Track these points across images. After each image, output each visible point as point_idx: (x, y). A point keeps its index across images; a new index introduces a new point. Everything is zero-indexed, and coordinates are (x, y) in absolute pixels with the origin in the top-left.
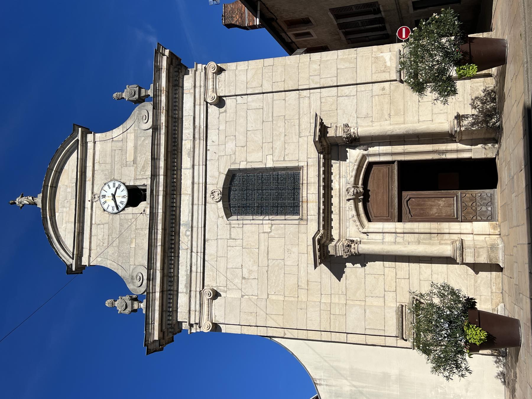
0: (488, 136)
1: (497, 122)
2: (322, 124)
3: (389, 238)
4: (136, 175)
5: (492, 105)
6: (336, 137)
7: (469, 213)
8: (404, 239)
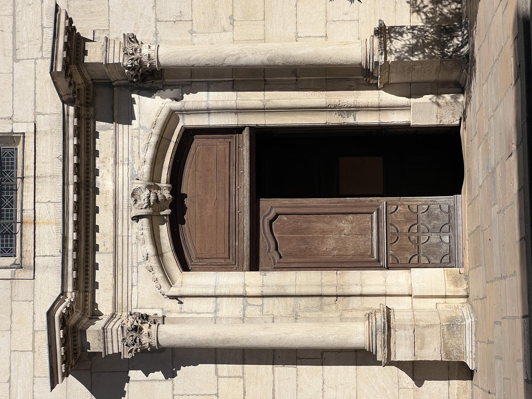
0: (443, 76)
1: (462, 47)
2: (71, 30)
3: (230, 308)
5: (453, 6)
6: (107, 65)
7: (402, 249)
8: (262, 311)
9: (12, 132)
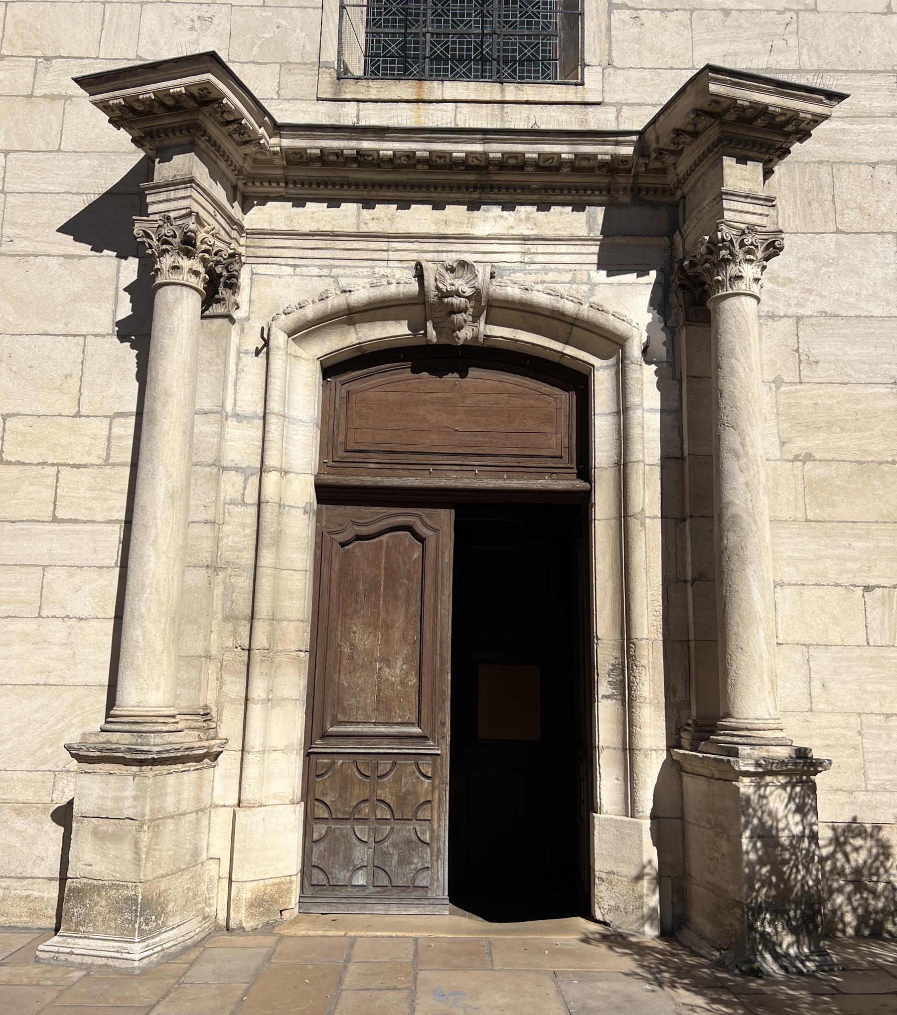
0: (699, 894)
1: (776, 957)
5: (849, 918)
6: (720, 196)
7: (345, 784)
8: (233, 503)
9: (585, 65)
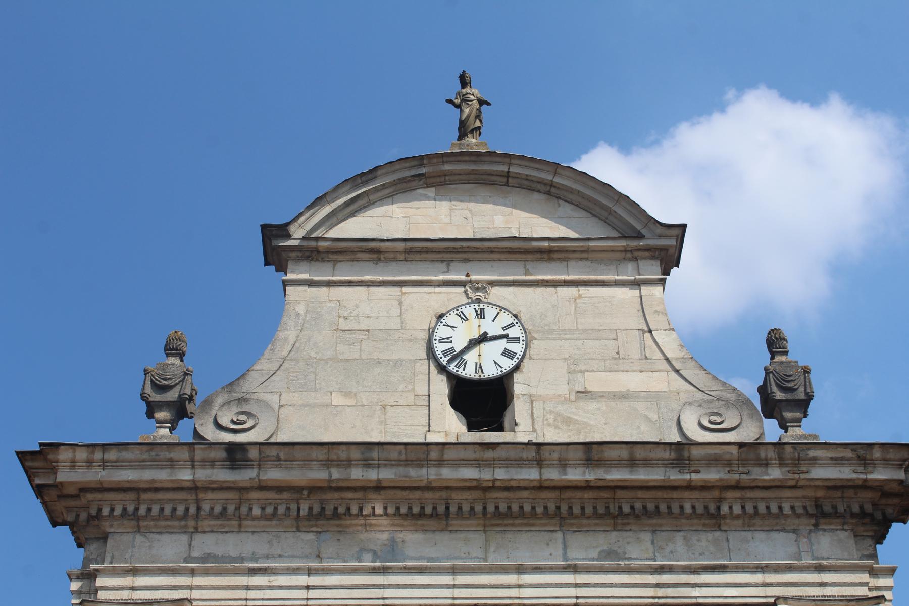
4: (545, 399)
